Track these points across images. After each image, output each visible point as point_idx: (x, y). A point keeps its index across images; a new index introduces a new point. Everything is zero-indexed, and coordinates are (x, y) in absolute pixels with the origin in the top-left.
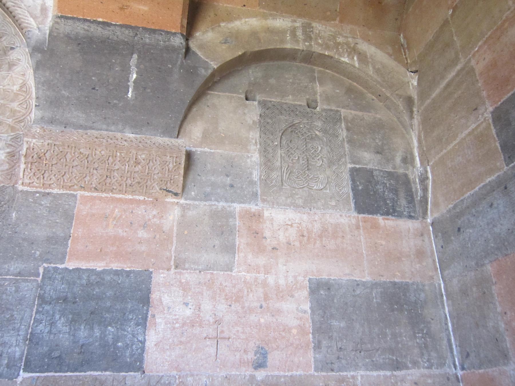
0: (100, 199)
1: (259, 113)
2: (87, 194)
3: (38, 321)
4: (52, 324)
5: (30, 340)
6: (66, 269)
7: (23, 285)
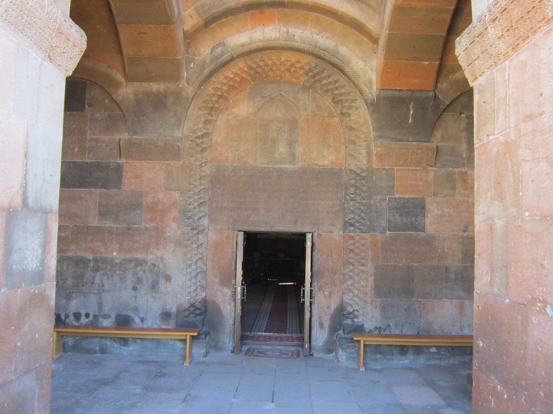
0: (403, 169)
1: (466, 122)
2: (398, 168)
3: (389, 216)
4: (394, 217)
5: (388, 222)
6: (395, 198)
7: (382, 204)
